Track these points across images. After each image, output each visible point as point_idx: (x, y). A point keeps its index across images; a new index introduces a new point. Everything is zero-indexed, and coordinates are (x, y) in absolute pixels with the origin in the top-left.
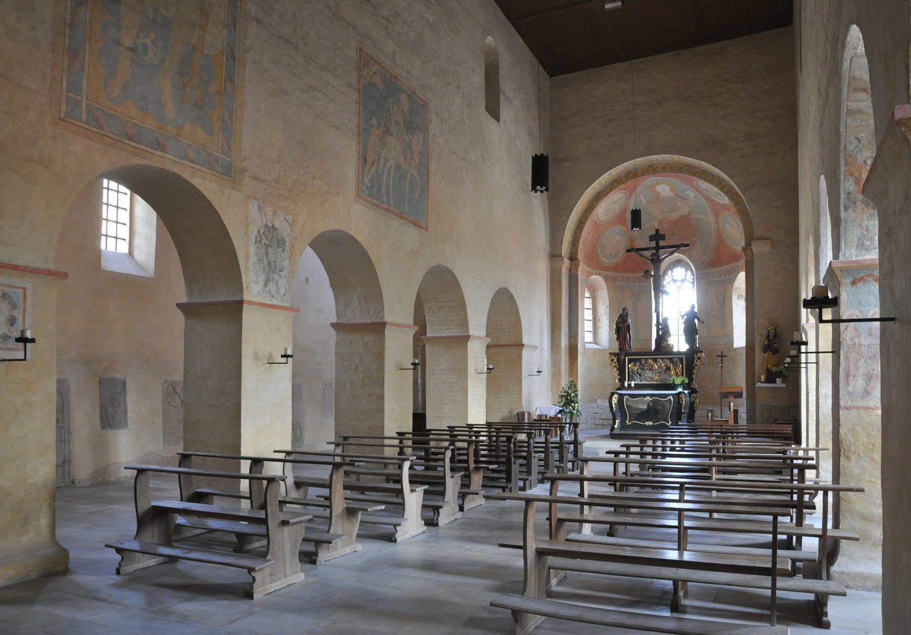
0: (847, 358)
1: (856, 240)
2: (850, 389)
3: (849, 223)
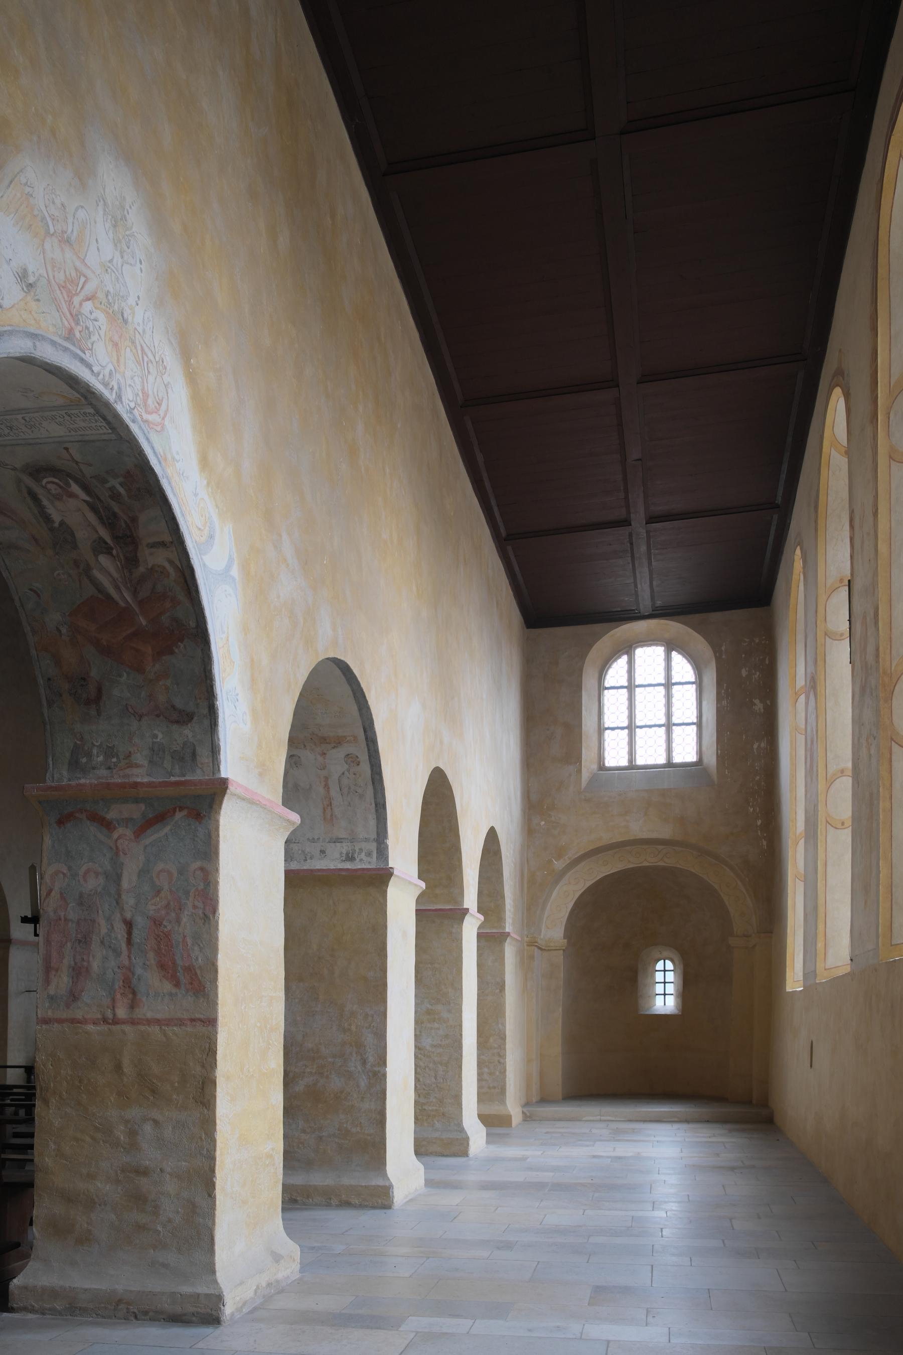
1: (68, 755)
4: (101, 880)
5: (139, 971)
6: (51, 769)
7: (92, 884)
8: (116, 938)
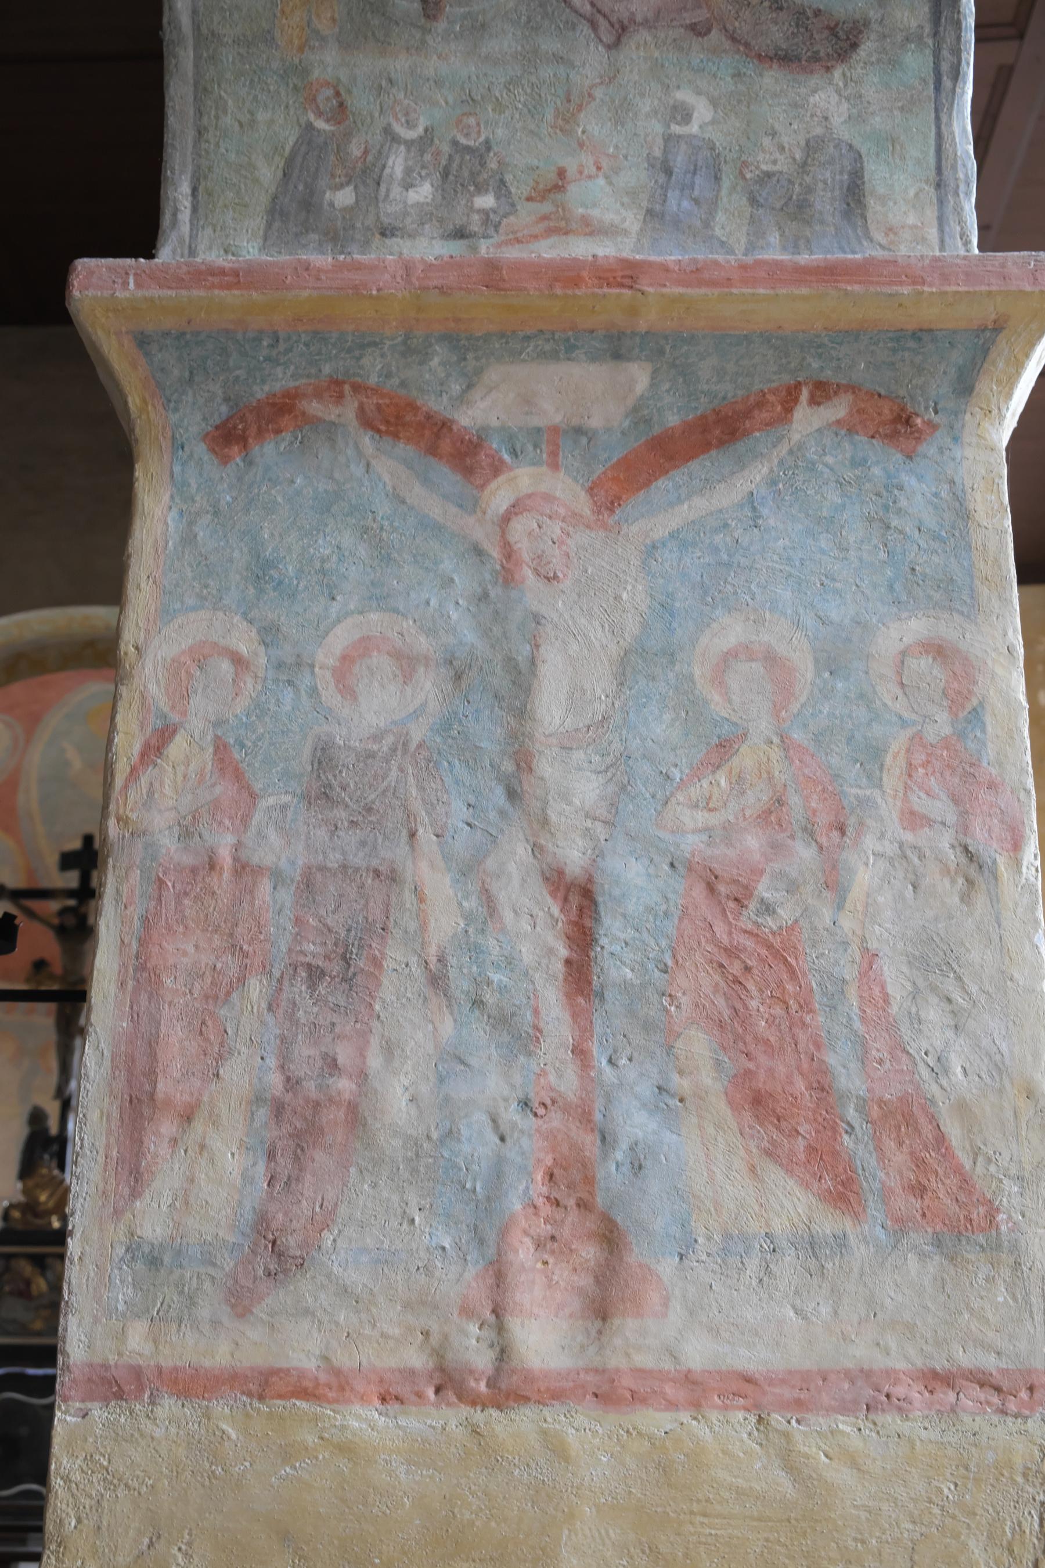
0: (143, 973)
1: (268, 174)
2: (152, 1221)
3: (228, 56)
4: (429, 688)
5: (635, 1123)
6: (185, 228)
7: (379, 707)
8: (510, 962)
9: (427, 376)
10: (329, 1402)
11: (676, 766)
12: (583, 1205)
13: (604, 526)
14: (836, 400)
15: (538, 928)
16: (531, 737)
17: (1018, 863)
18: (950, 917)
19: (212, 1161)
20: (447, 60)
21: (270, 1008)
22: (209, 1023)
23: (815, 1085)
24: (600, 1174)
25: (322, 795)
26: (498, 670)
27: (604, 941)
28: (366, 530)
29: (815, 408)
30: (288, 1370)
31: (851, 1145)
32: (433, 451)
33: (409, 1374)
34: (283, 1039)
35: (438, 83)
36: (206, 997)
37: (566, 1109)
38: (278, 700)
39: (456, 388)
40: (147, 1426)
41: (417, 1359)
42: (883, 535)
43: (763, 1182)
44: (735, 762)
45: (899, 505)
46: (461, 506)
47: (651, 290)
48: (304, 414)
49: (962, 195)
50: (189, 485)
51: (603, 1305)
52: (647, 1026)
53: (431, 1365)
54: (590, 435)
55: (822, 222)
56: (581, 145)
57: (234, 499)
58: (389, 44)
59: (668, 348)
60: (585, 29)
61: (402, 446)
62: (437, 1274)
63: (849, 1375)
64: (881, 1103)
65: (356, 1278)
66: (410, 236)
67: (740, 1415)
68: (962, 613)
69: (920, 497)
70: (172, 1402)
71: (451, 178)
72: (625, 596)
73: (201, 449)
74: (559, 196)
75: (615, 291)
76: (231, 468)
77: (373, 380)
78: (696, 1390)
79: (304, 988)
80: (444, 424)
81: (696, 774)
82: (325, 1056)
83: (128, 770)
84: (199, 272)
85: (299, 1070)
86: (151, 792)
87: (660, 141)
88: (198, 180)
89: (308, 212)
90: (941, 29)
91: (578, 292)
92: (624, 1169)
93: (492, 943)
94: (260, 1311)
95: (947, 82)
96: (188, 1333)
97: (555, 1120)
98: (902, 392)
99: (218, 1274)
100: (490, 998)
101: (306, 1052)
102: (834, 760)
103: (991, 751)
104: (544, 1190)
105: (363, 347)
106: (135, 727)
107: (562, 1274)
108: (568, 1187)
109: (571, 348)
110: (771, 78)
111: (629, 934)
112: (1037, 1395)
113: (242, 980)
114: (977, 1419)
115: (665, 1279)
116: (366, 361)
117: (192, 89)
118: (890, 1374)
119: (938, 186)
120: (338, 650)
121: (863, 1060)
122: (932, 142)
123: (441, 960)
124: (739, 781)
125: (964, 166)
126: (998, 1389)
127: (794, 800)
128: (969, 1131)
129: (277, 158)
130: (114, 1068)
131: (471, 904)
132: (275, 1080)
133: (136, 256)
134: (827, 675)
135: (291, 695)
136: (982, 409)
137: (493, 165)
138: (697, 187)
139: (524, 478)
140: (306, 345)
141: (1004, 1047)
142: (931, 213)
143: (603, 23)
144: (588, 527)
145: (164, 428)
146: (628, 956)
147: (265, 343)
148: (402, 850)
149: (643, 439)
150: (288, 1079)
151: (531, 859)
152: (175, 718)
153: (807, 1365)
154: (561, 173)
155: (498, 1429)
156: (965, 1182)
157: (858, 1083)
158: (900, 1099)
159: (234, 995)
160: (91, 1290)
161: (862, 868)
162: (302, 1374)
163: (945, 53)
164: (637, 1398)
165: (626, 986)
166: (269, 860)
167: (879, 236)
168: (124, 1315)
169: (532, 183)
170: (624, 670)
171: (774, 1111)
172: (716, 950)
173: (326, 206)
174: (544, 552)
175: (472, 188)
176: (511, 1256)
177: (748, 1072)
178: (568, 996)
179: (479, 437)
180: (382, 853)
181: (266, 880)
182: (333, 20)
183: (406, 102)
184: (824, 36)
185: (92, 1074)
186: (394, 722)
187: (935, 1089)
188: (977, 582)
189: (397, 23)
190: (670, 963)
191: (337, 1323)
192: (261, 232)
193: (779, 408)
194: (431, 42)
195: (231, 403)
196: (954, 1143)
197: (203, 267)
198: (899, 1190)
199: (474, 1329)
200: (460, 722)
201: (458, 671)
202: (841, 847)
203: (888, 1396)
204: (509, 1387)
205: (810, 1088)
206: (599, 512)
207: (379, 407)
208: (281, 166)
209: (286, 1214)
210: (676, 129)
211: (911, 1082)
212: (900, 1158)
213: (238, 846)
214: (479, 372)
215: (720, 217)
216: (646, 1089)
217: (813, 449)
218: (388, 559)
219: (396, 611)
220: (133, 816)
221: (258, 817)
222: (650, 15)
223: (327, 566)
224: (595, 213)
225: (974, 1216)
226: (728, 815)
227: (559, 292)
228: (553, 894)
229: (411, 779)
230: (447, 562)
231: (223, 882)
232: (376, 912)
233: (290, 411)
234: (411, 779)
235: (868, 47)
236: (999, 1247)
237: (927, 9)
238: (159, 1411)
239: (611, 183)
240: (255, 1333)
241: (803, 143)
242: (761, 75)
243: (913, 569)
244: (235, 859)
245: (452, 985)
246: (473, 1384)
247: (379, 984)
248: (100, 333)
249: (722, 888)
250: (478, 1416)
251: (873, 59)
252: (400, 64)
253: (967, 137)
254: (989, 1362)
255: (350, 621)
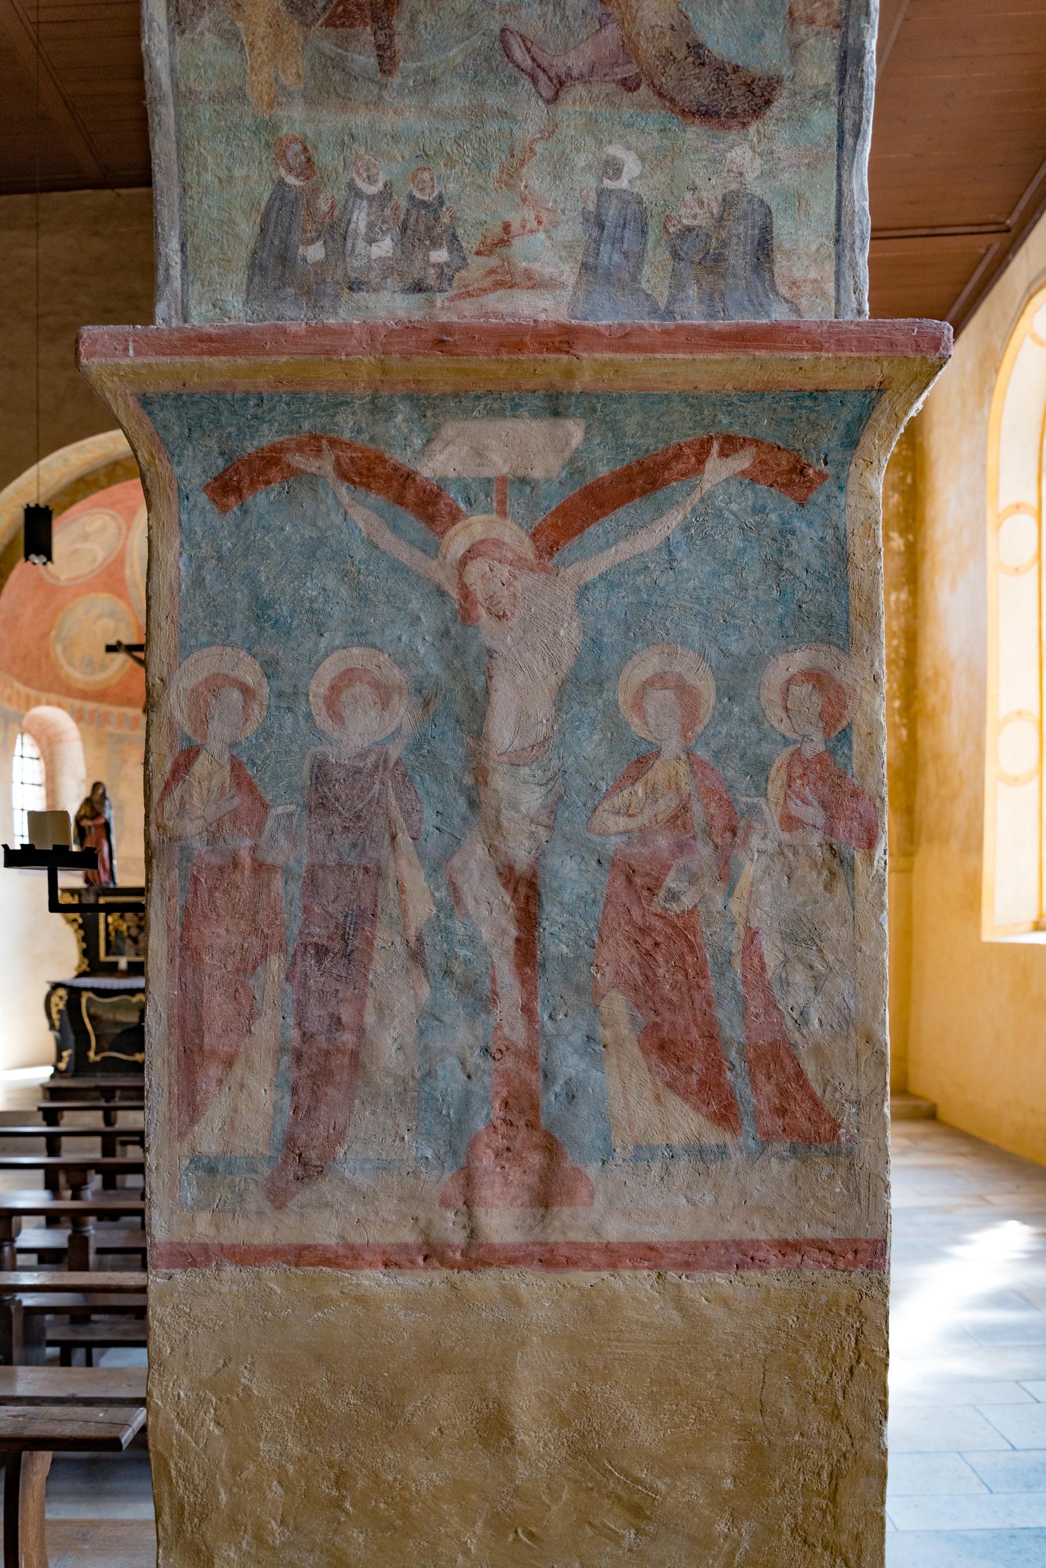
1: (247, 229)
2: (208, 1138)
3: (206, 112)
4: (402, 713)
5: (570, 1064)
6: (177, 284)
7: (365, 729)
8: (472, 940)
9: (393, 432)
10: (346, 1268)
11: (603, 779)
12: (530, 1125)
13: (545, 569)
14: (741, 453)
15: (494, 914)
16: (487, 756)
17: (871, 858)
18: (816, 902)
19: (250, 1095)
20: (402, 115)
21: (287, 979)
22: (241, 990)
23: (706, 1034)
24: (543, 1103)
25: (320, 805)
26: (459, 698)
27: (545, 924)
28: (346, 573)
29: (724, 459)
30: (316, 1246)
31: (732, 1079)
32: (400, 500)
33: (404, 1247)
34: (299, 1002)
35: (395, 138)
36: (238, 970)
37: (518, 1054)
38: (280, 725)
39: (418, 442)
40: (216, 1285)
41: (409, 1236)
42: (777, 576)
43: (666, 1106)
44: (650, 775)
45: (791, 549)
46: (424, 551)
47: (585, 355)
48: (289, 466)
49: (857, 251)
50: (195, 533)
51: (545, 1196)
52: (578, 989)
53: (420, 1241)
54: (533, 484)
55: (735, 276)
56: (524, 200)
57: (235, 545)
58: (350, 99)
59: (599, 406)
60: (526, 83)
61: (373, 496)
62: (423, 1177)
63: (724, 1244)
64: (756, 1047)
65: (363, 1181)
66: (374, 290)
67: (645, 1273)
68: (838, 646)
69: (808, 541)
70: (233, 1268)
71: (409, 232)
72: (562, 632)
73: (203, 499)
74: (504, 250)
75: (553, 356)
76: (230, 515)
77: (347, 436)
78: (614, 1256)
79: (313, 962)
80: (409, 475)
81: (618, 787)
82: (331, 1016)
83: (163, 785)
84: (190, 338)
85: (312, 1027)
86: (182, 804)
87: (593, 195)
88: (185, 235)
89: (284, 267)
90: (846, 87)
91: (521, 357)
92: (561, 1098)
93: (458, 925)
94: (293, 1205)
95: (849, 141)
96: (241, 1221)
97: (509, 1062)
98: (798, 446)
99: (260, 1179)
100: (458, 969)
101: (318, 1013)
102: (730, 774)
103: (855, 764)
104: (501, 1114)
105: (337, 405)
106: (165, 749)
107: (515, 1175)
108: (520, 1113)
109: (515, 407)
110: (693, 134)
111: (564, 918)
112: (859, 1256)
113: (264, 956)
114: (816, 1273)
115: (591, 1178)
116: (339, 419)
117: (175, 146)
118: (756, 1244)
119: (837, 241)
120: (327, 683)
121: (744, 1013)
122: (834, 192)
123: (419, 939)
124: (652, 790)
125: (861, 222)
126: (832, 1253)
127: (697, 807)
128: (822, 1068)
129: (254, 214)
130: (170, 1026)
131: (442, 894)
132: (294, 1034)
133: (133, 322)
134: (726, 700)
135: (291, 720)
136: (865, 460)
137: (446, 220)
138: (626, 241)
139: (476, 526)
140: (288, 404)
141: (852, 1004)
142: (830, 268)
143: (543, 79)
144: (532, 570)
145: (170, 481)
146: (565, 935)
147: (252, 403)
148: (386, 851)
149: (578, 489)
150: (304, 1034)
151: (488, 858)
152: (197, 740)
153: (696, 1236)
154: (506, 227)
155: (470, 1285)
156: (817, 1104)
157: (739, 1032)
158: (771, 1044)
159: (259, 968)
160: (167, 1190)
161: (748, 863)
162: (326, 1248)
163: (848, 111)
164: (571, 1263)
165: (562, 959)
166: (280, 860)
167: (783, 290)
168: (192, 1208)
169: (480, 238)
170: (561, 697)
171: (674, 1053)
172: (633, 930)
173: (299, 262)
174: (495, 593)
175: (428, 243)
176: (477, 1163)
177: (656, 1025)
178: (518, 966)
179: (439, 487)
180: (370, 853)
181: (278, 876)
182: (299, 76)
183: (367, 157)
184: (741, 92)
185: (153, 1031)
186: (376, 743)
187: (797, 1036)
188: (852, 618)
189: (356, 79)
190: (597, 940)
191: (350, 1213)
192: (244, 287)
193: (693, 460)
194: (387, 97)
195: (226, 457)
196: (810, 1077)
197: (192, 334)
198: (767, 1112)
199: (450, 1215)
200: (429, 742)
201: (425, 698)
202: (733, 846)
203: (752, 1259)
204: (477, 1256)
205: (702, 1036)
206: (541, 557)
207: (352, 459)
208: (258, 221)
209: (308, 1135)
210: (608, 183)
211: (780, 1031)
212: (769, 1088)
213: (255, 849)
214: (436, 428)
215: (647, 270)
216: (577, 1038)
217: (721, 497)
218: (364, 599)
219: (373, 646)
220: (170, 824)
221: (270, 824)
222: (585, 70)
223: (315, 606)
224: (536, 266)
225: (822, 1131)
226: (642, 820)
227: (505, 358)
228: (505, 885)
229: (390, 790)
230: (414, 602)
231: (244, 878)
232: (367, 901)
233: (277, 464)
234: (390, 790)
235: (781, 103)
236: (839, 1153)
237: (834, 67)
238: (223, 1275)
239: (550, 237)
240: (291, 1220)
241: (720, 198)
242: (684, 131)
243: (800, 607)
244: (254, 859)
245: (428, 959)
246: (451, 1254)
247: (371, 960)
248: (108, 395)
249: (638, 881)
250: (455, 1276)
251: (785, 116)
252: (360, 120)
253: (864, 194)
254: (827, 1234)
255: (336, 655)
